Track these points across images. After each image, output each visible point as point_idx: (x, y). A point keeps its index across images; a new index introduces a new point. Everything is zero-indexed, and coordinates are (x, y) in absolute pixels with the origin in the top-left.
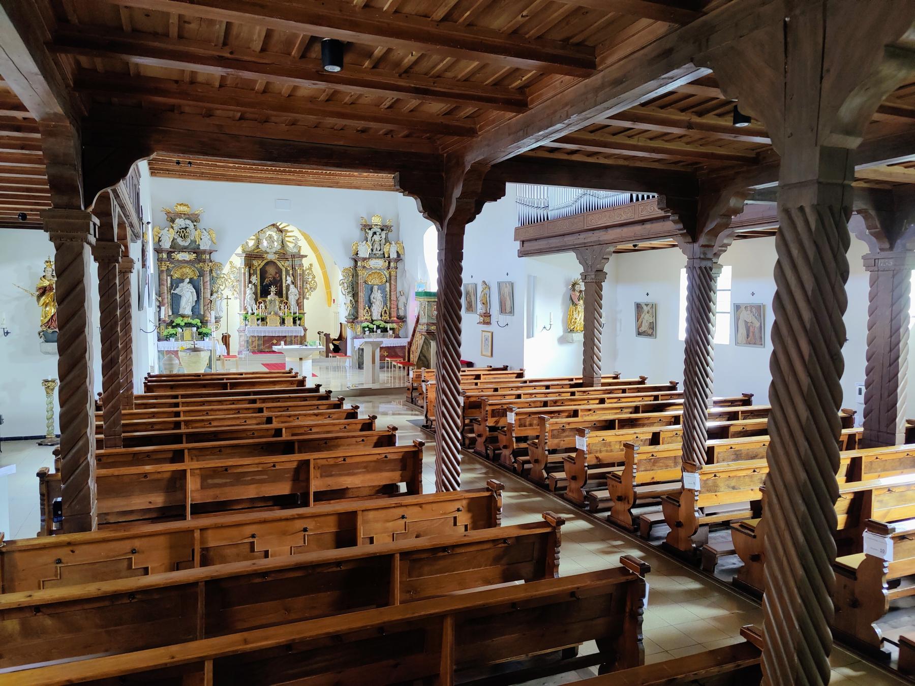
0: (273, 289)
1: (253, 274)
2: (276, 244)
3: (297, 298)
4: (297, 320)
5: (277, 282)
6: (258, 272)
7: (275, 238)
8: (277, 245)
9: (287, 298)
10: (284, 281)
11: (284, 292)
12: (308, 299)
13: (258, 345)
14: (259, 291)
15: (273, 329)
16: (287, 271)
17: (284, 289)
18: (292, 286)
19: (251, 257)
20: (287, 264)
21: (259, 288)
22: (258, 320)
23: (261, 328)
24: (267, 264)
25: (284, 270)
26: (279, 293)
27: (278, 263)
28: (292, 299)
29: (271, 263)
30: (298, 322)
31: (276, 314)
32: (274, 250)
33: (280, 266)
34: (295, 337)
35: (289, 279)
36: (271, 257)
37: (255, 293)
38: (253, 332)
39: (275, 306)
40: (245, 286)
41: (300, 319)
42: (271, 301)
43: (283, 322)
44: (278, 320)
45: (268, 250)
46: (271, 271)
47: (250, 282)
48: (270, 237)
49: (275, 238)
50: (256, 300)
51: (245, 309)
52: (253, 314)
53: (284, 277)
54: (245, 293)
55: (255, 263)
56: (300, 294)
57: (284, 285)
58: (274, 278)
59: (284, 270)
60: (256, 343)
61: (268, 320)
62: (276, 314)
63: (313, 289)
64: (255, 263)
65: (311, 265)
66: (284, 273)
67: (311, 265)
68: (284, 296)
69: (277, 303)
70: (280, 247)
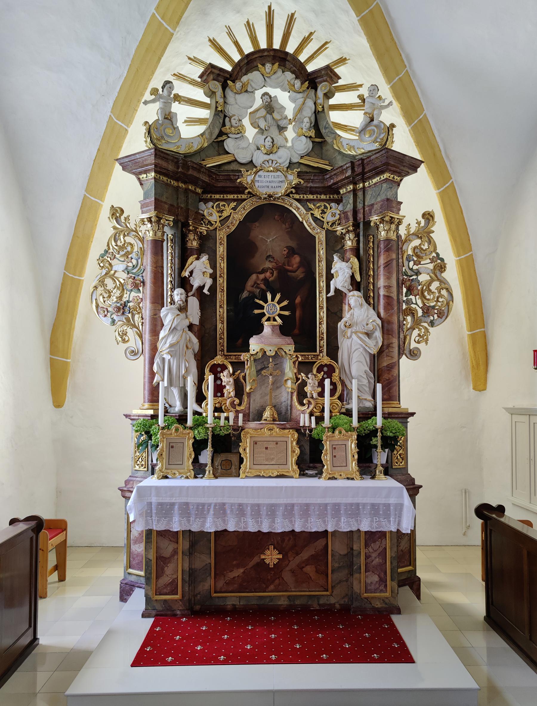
0: (272, 308)
1: (199, 252)
2: (290, 133)
3: (375, 344)
4: (380, 446)
5: (298, 286)
6: (221, 250)
7: (290, 113)
8: (294, 142)
9: (333, 351)
10: (321, 283)
11: (322, 328)
12: (414, 355)
13: (192, 577)
14: (222, 327)
15: (264, 495)
16: (334, 243)
17: (321, 314)
18: (354, 298)
19: (186, 181)
20: (332, 213)
21: (222, 311)
22: (199, 446)
23: (212, 486)
24: (256, 215)
25: (321, 237)
26: (299, 329)
27: (299, 212)
28: (355, 351)
29: (270, 211)
30: (380, 457)
31: (284, 418)
32: (283, 157)
33: (309, 225)
34: (373, 537)
35: (343, 271)
36: (271, 183)
37: (204, 332)
38: (165, 510)
39: (277, 384)
40: (158, 300)
41: (391, 442)
42: (262, 361)
43: (311, 459)
44: (293, 452)
45: (259, 158)
46: (272, 242)
47: (184, 283)
48: (270, 106)
49: (290, 113)
50: (203, 357)
51: (153, 395)
52: (182, 419)
53: (321, 267)
54: (156, 325)
55: (211, 212)
56: (386, 328)
57: (321, 299)
58: (282, 271)
59: (321, 237)
60: (176, 570)
61: (246, 448)
62: (284, 418)
63: (437, 313)
64: (211, 212)
65: (428, 217)
66: (321, 251)
67: (428, 217)
68: (322, 343)
69: (289, 369)
70: (304, 145)
